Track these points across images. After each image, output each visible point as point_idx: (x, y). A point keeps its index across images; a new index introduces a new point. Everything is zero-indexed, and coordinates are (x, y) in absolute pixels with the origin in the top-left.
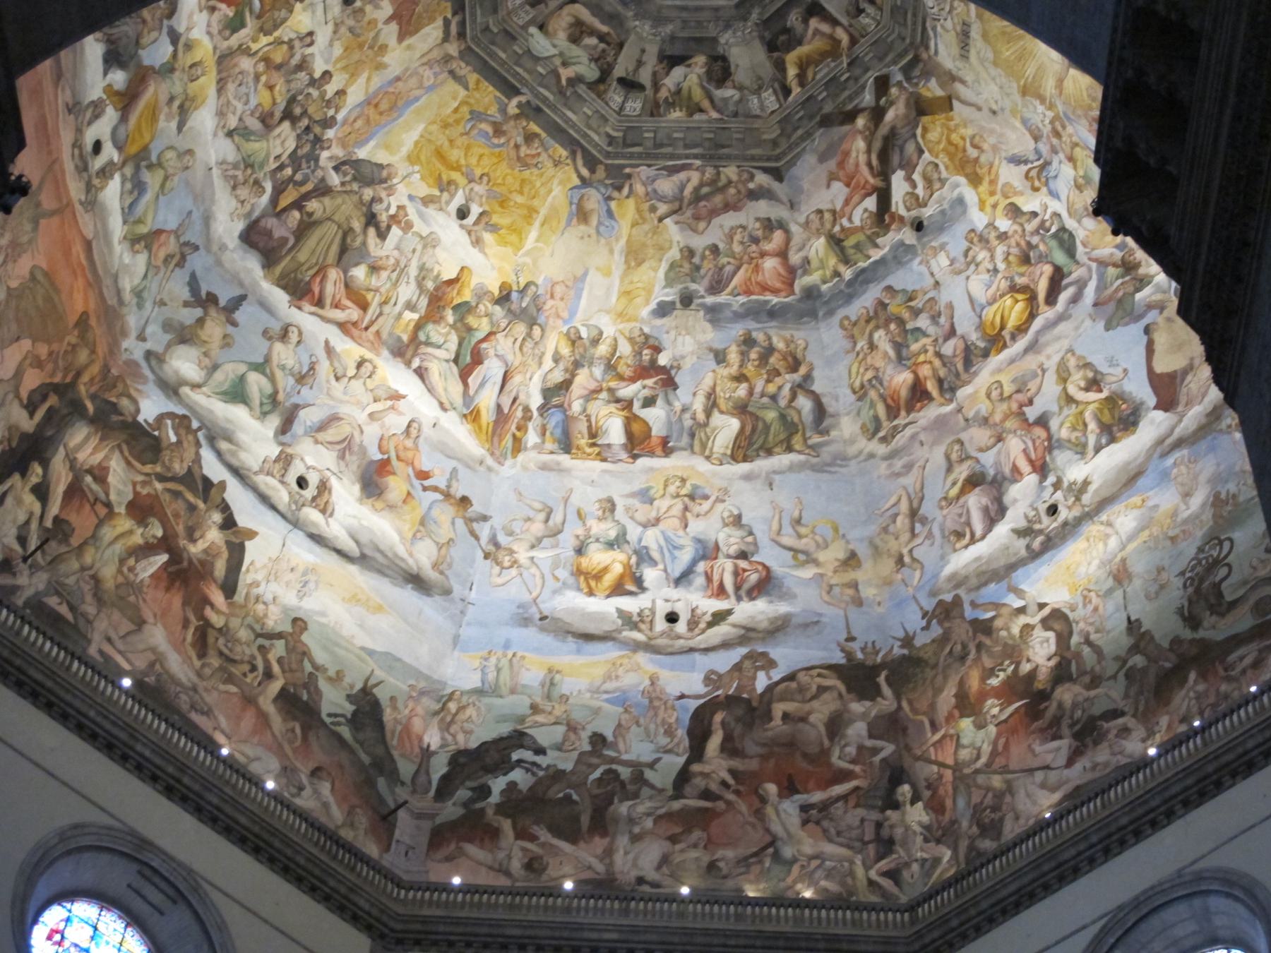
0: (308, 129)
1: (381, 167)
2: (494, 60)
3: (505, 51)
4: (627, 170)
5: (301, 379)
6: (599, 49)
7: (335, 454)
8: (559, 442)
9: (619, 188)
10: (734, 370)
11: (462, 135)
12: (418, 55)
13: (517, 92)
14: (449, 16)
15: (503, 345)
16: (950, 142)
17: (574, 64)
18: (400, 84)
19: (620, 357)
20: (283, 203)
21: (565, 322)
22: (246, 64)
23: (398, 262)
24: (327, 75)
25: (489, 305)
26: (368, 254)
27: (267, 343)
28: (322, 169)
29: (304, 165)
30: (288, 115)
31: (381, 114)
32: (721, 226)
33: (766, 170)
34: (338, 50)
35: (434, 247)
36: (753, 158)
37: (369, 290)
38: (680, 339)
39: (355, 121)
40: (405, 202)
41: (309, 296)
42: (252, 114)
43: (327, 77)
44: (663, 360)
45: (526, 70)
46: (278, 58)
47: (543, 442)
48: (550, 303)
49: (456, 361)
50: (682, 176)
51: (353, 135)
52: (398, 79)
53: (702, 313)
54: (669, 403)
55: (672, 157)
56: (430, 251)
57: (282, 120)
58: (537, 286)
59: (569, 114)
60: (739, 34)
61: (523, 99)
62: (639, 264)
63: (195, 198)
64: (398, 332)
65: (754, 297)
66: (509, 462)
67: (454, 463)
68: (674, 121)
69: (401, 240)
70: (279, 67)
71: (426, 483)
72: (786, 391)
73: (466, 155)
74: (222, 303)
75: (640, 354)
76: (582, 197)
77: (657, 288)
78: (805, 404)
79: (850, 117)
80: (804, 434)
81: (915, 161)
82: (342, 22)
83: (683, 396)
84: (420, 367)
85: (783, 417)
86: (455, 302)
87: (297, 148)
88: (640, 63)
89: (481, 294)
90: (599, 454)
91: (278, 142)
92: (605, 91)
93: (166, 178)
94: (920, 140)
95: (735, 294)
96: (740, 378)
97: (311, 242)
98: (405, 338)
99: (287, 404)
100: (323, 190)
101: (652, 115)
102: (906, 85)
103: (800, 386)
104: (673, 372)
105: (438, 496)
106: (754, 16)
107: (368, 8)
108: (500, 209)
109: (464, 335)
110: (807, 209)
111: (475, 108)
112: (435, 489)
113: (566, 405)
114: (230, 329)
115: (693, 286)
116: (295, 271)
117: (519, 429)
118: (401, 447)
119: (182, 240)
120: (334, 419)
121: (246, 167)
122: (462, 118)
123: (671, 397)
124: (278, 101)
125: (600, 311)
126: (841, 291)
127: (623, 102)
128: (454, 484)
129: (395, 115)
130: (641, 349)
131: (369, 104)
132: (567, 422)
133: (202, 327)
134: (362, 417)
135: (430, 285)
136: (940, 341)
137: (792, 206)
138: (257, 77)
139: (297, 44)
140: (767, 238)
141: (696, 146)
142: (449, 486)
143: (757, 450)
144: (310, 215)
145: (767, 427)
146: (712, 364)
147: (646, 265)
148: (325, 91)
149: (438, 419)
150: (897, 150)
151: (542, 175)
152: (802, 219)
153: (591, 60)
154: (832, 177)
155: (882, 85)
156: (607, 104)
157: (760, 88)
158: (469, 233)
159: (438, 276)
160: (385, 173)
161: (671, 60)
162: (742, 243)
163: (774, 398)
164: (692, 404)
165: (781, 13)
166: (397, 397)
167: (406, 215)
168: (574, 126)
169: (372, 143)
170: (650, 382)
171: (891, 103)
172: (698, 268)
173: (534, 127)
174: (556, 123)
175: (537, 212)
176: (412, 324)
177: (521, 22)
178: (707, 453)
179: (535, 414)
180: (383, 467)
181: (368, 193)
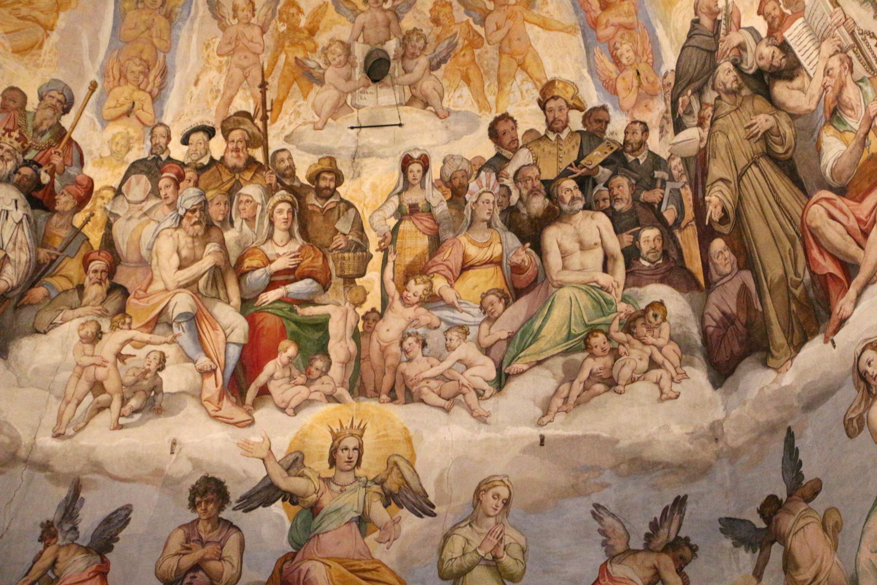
0: (585, 182)
1: (696, 22)
37: (863, 142)
39: (616, 61)
41: (833, 290)
42: (491, 319)
43: (502, 127)
51: (642, 68)
57: (538, 247)
63: (576, 491)
69: (808, 25)
70: (436, 243)
74: (781, 493)
87: (612, 214)
91: (576, 260)
93: (494, 564)
107: (408, 23)
114: (819, 504)
116: (790, 296)
119: (637, 543)
121: (587, 347)
124: (497, 250)
131: (595, 24)
133: (797, 567)
138: (432, 300)
139: (413, 197)
144: (724, 219)
160: (706, 22)
169: (660, 32)
181: (726, 74)
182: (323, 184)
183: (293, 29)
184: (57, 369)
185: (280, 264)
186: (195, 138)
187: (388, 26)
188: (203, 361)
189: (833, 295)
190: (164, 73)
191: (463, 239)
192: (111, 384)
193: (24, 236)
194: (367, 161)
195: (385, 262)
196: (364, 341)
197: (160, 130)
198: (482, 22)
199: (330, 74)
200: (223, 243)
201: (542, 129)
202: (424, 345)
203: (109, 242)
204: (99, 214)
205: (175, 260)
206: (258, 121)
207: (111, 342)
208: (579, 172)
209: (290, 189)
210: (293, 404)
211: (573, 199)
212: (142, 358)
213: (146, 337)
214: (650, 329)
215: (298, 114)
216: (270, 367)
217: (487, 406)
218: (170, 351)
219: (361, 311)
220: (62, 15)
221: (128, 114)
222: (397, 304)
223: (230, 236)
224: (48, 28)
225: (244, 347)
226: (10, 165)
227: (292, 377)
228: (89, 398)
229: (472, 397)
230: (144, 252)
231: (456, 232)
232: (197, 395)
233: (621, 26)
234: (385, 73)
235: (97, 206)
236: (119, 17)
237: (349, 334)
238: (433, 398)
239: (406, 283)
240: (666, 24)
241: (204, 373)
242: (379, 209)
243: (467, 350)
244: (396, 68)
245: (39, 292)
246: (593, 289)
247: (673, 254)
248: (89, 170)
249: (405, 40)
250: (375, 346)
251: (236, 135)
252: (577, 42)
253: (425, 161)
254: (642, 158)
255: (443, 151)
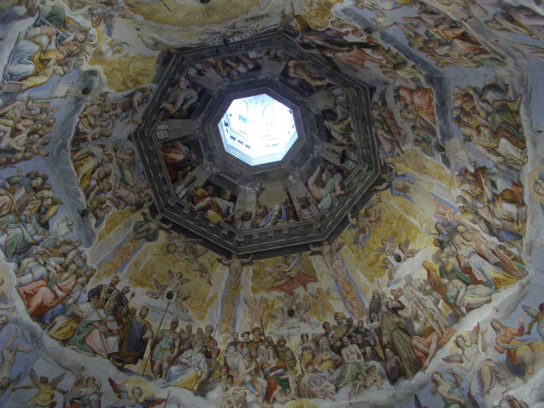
0: (350, 337)
1: (373, 297)
2: (332, 227)
3: (329, 222)
4: (382, 164)
5: (457, 384)
6: (328, 172)
7: (497, 384)
8: (516, 239)
9: (391, 170)
10: (474, 133)
11: (364, 251)
12: (326, 269)
13: (346, 217)
14: (309, 252)
15: (464, 251)
16: (317, 16)
17: (334, 186)
18: (339, 279)
19: (472, 191)
20: (382, 355)
21: (456, 212)
22: (305, 379)
23: (415, 303)
24: (325, 326)
25: (443, 255)
26: (409, 318)
27: (438, 394)
28: (371, 329)
29: (367, 339)
30: (338, 351)
31: (352, 291)
32: (402, 122)
33: (372, 96)
34: (314, 319)
35: (411, 279)
36: (367, 101)
37: (425, 324)
38: (460, 157)
39: (352, 306)
40: (389, 289)
42: (331, 374)
43: (326, 325)
44: (472, 170)
45: (337, 212)
46: (308, 356)
47: (517, 247)
48: (447, 216)
49: (467, 284)
50: (381, 138)
52: (336, 281)
53: (446, 142)
54: (494, 174)
55: (373, 141)
56: (413, 282)
57: (340, 355)
58: (438, 223)
59: (357, 191)
60: (311, 104)
61: (350, 215)
62: (426, 168)
64: (447, 315)
65: (435, 112)
66: (527, 269)
67: (520, 306)
68: (356, 138)
69: (405, 297)
70: (314, 356)
71: (526, 331)
72: (484, 105)
73: (373, 250)
75: (469, 180)
76: (396, 188)
77: (436, 162)
78: (490, 96)
79: (329, 60)
80: (508, 101)
81: (335, 32)
82: (301, 317)
83: (489, 165)
84: (466, 308)
85: (498, 111)
86: (439, 275)
87: (358, 345)
88: (333, 151)
89: (437, 258)
90: (522, 222)
91: (351, 357)
92: (347, 170)
94: (323, 29)
95: (435, 123)
96: (478, 130)
97: (400, 347)
98: (451, 312)
99: (467, 399)
100: (379, 331)
101: (355, 148)
102: (300, 36)
103: (480, 96)
104: (478, 166)
105: (535, 325)
106: (300, 98)
107: (297, 301)
108: (399, 237)
109: (455, 275)
110: (386, 78)
111: (352, 241)
112: (531, 325)
113: (498, 227)
115: (433, 143)
117: (510, 255)
118: (503, 338)
120: (480, 374)
121: (357, 378)
122: (357, 249)
123: (490, 171)
124: (330, 356)
125: (449, 193)
126: (422, 66)
127: (352, 161)
128: (531, 311)
129: (353, 284)
130: (466, 179)
131: (345, 298)
132: (504, 229)
134: (483, 356)
135: (428, 288)
136: (427, 24)
137: (386, 83)
138: (315, 371)
139: (306, 345)
140: (404, 100)
141: (366, 129)
142: (532, 316)
143: (518, 132)
144: (388, 343)
145: (505, 122)
146: (472, 144)
147: (425, 164)
148: (333, 326)
149: (494, 307)
150: (334, 39)
151: (385, 210)
152: (391, 80)
153: (333, 177)
154: (363, 66)
155: (306, 46)
156: (353, 170)
157: (334, 95)
158: (408, 257)
159: (424, 281)
160: (376, 296)
161: (329, 138)
162: (408, 113)
163: (488, 114)
164: (494, 162)
165: (294, 88)
166: (477, 328)
167: (395, 290)
168: (362, 189)
169: (363, 299)
170: (483, 181)
171: (312, 42)
172: (424, 139)
173: (362, 211)
174: (360, 199)
175: (402, 215)
176: (445, 305)
177: (317, 212)
178: (521, 163)
179: (501, 243)
180: (511, 355)
181: (384, 308)
182: (281, 344)
183: (267, 305)
184: (218, 399)
185: (273, 365)
186: (245, 335)
187: (292, 303)
188: (257, 393)
189: (423, 361)
190: (235, 319)
191: (320, 354)
192: (233, 401)
193: (206, 365)
194: (292, 337)
195: (301, 362)
196: (299, 383)
197: (235, 334)
198: (317, 299)
199: (279, 316)
200: (256, 362)
201: (336, 325)
202: (315, 382)
203: (226, 364)
204: (222, 357)
205: (244, 367)
206: (261, 330)
207: (231, 390)
208: (347, 335)
209: (273, 346)
210: (283, 401)
211: (347, 342)
212: (240, 393)
213: (240, 388)
214: (372, 372)
215: (271, 327)
216: (275, 393)
217: (335, 396)
218: (247, 391)
219: (297, 376)
220: (209, 308)
221: (226, 331)
222: (306, 373)
223: (258, 359)
224: (206, 312)
225: (267, 388)
226: (200, 348)
227: (281, 395)
228: (228, 406)
229: (330, 395)
230: (236, 366)
231: (318, 353)
232: (257, 402)
233: (352, 298)
234: (293, 314)
235: (222, 355)
236: (222, 307)
237: (295, 381)
238: (320, 396)
239: (307, 367)
240: (365, 297)
241: (258, 396)
242: (297, 349)
243: (327, 383)
244: (296, 313)
245: (211, 379)
246: (356, 363)
247: (375, 353)
248: (219, 346)
249: (297, 306)
250: (302, 384)
251: (256, 333)
252: (341, 303)
253: (307, 336)
254: (363, 330)
255: (312, 332)
